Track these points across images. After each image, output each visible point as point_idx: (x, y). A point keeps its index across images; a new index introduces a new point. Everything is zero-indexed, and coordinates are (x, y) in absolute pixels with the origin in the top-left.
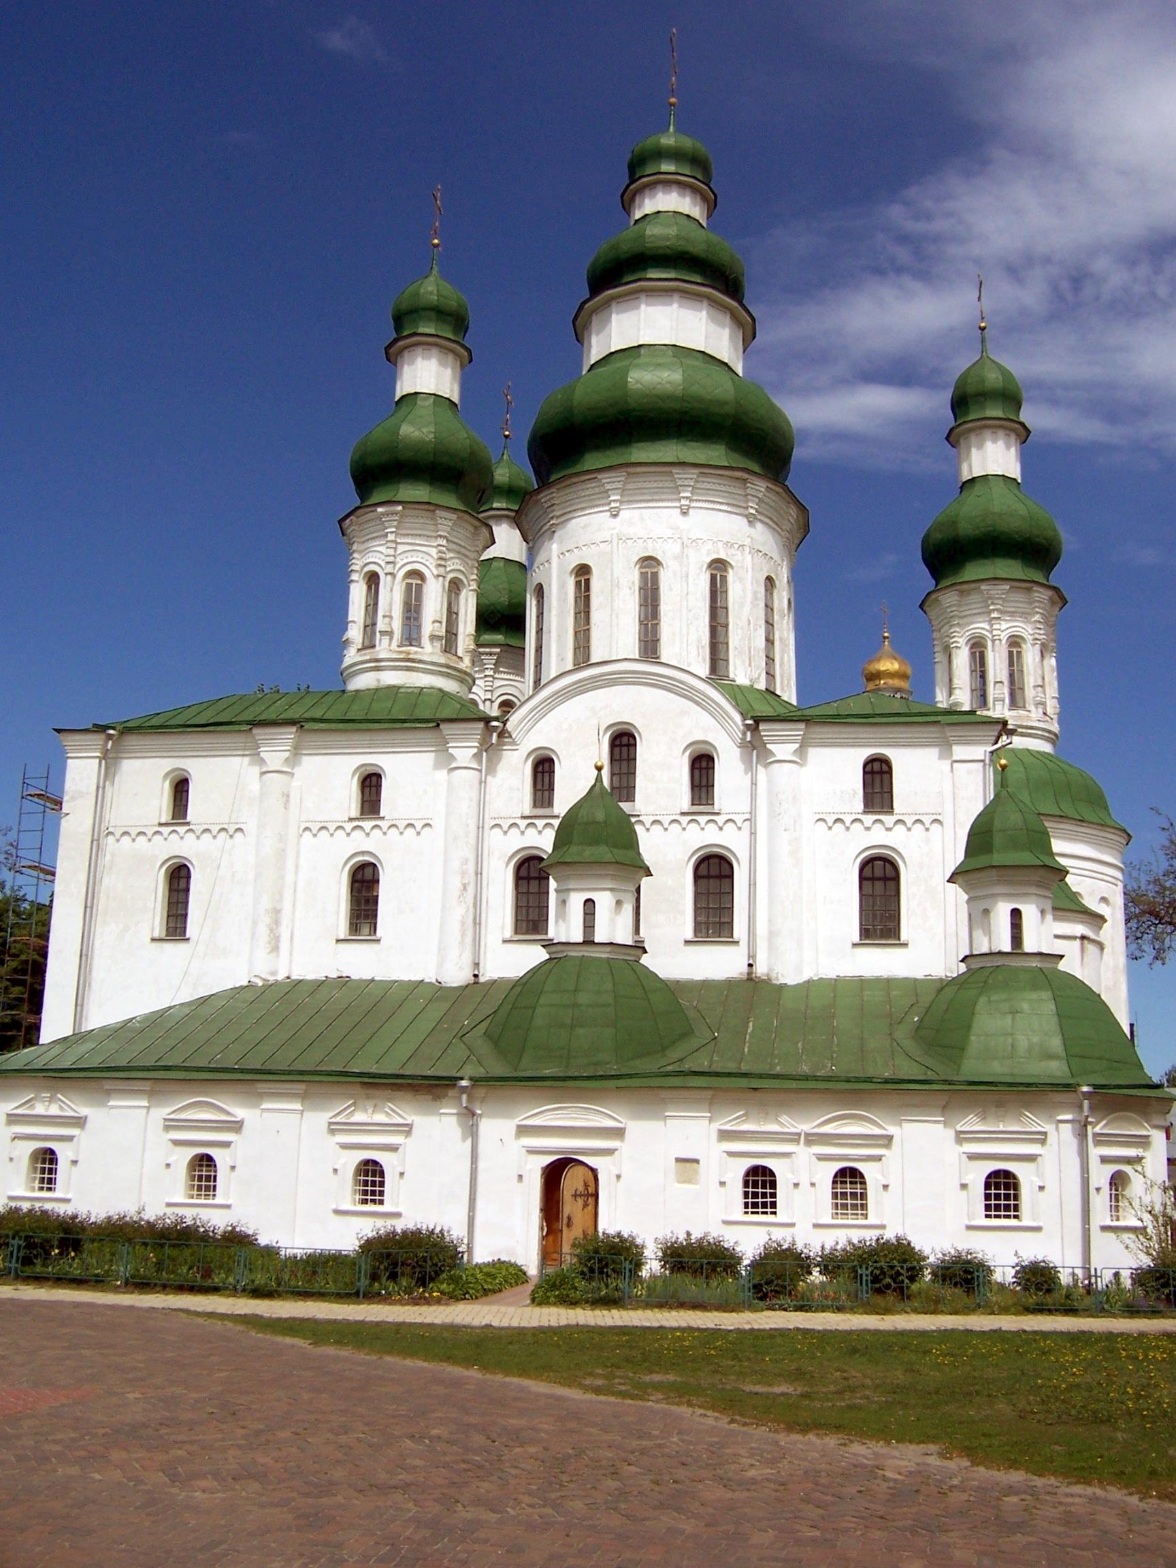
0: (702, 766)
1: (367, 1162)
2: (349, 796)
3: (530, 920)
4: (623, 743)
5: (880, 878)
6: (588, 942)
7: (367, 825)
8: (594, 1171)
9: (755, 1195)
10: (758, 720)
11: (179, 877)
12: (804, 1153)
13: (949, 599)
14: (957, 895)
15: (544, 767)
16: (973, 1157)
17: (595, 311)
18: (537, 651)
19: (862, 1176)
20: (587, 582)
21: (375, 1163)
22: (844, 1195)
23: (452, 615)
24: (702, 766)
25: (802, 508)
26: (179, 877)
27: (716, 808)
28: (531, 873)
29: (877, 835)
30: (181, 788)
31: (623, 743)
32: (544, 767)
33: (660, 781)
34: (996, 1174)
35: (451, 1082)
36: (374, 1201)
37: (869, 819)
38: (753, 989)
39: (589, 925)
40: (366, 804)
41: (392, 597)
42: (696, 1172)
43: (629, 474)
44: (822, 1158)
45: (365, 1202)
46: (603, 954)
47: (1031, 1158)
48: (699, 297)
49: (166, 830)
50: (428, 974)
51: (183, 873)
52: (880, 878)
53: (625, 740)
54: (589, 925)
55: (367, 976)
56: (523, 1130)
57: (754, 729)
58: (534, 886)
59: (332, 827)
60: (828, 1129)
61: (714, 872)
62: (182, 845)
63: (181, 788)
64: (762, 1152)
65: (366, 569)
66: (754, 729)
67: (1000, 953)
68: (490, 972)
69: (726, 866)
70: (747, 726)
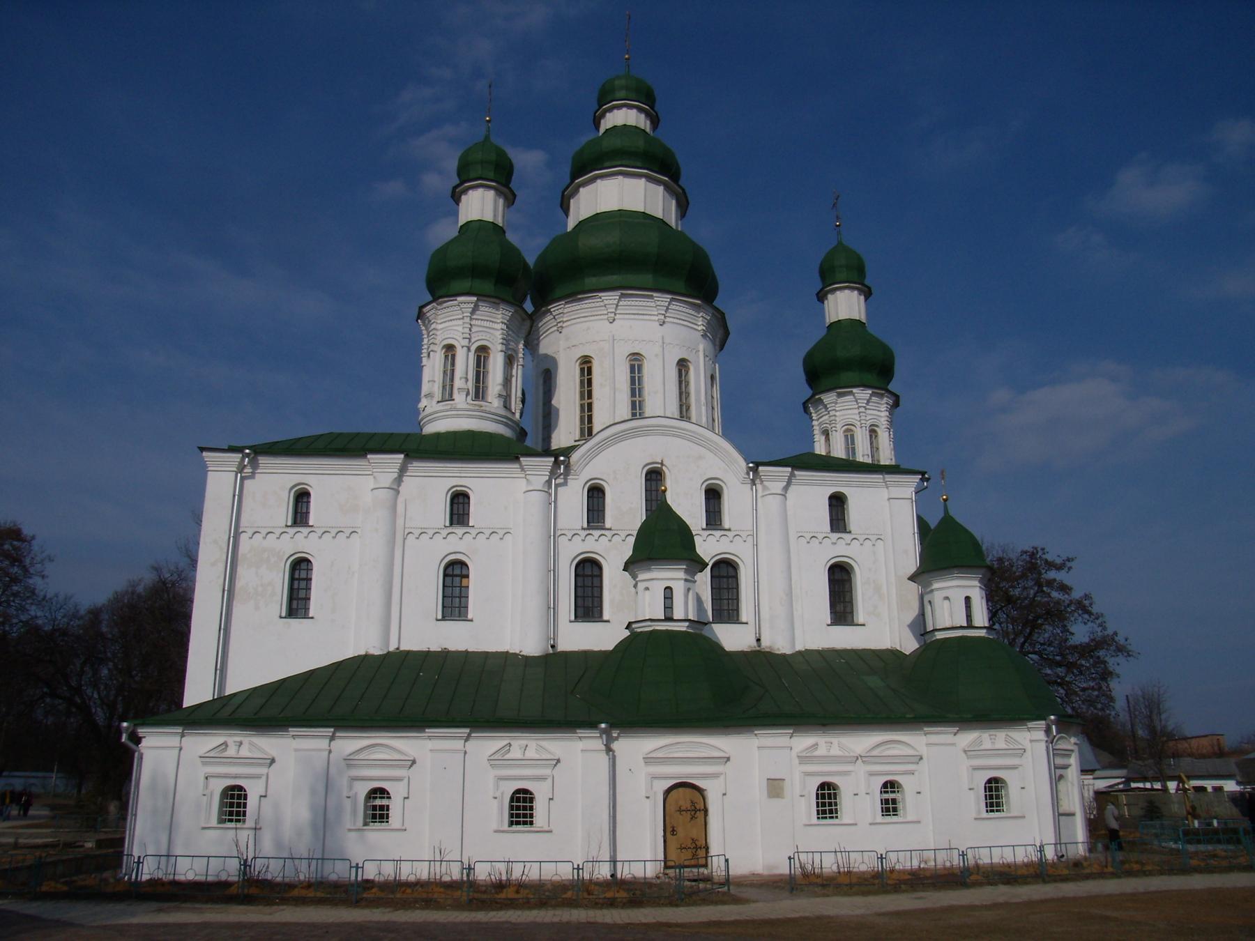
0: (713, 495)
1: (518, 791)
2: (440, 510)
3: (588, 606)
4: (654, 477)
5: (840, 577)
6: (669, 619)
7: (460, 531)
8: (700, 791)
9: (824, 804)
10: (758, 464)
11: (300, 569)
12: (861, 769)
13: (829, 398)
14: (914, 588)
15: (596, 494)
16: (976, 768)
17: (584, 184)
18: (544, 417)
19: (899, 786)
20: (590, 370)
21: (526, 791)
22: (887, 801)
23: (507, 382)
24: (713, 495)
25: (727, 333)
26: (300, 569)
27: (727, 526)
28: (588, 571)
29: (838, 548)
30: (302, 497)
31: (654, 477)
32: (596, 494)
33: (687, 504)
34: (989, 781)
35: (593, 725)
36: (525, 823)
37: (835, 536)
38: (760, 659)
39: (668, 607)
40: (455, 517)
41: (464, 363)
42: (782, 789)
43: (623, 296)
44: (872, 774)
45: (518, 823)
46: (682, 627)
47: (1014, 768)
48: (658, 182)
49: (292, 531)
50: (514, 648)
51: (304, 566)
52: (840, 577)
53: (654, 476)
54: (668, 607)
55: (462, 648)
56: (648, 760)
57: (755, 470)
58: (588, 582)
59: (431, 532)
60: (875, 753)
61: (725, 571)
62: (301, 543)
63: (302, 497)
64: (828, 772)
65: (446, 342)
66: (755, 470)
67: (962, 627)
68: (564, 645)
69: (731, 569)
70: (751, 469)
